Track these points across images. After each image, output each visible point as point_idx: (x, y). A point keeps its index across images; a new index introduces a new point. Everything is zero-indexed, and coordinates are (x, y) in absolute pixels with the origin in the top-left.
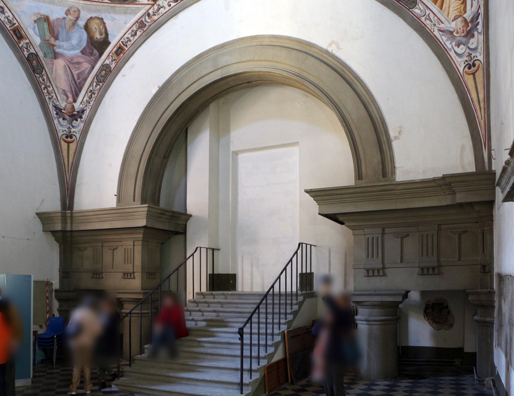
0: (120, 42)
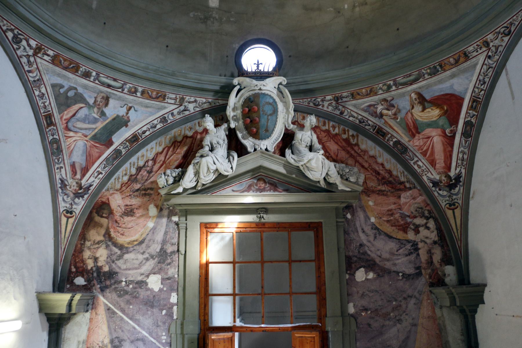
0: (137, 132)
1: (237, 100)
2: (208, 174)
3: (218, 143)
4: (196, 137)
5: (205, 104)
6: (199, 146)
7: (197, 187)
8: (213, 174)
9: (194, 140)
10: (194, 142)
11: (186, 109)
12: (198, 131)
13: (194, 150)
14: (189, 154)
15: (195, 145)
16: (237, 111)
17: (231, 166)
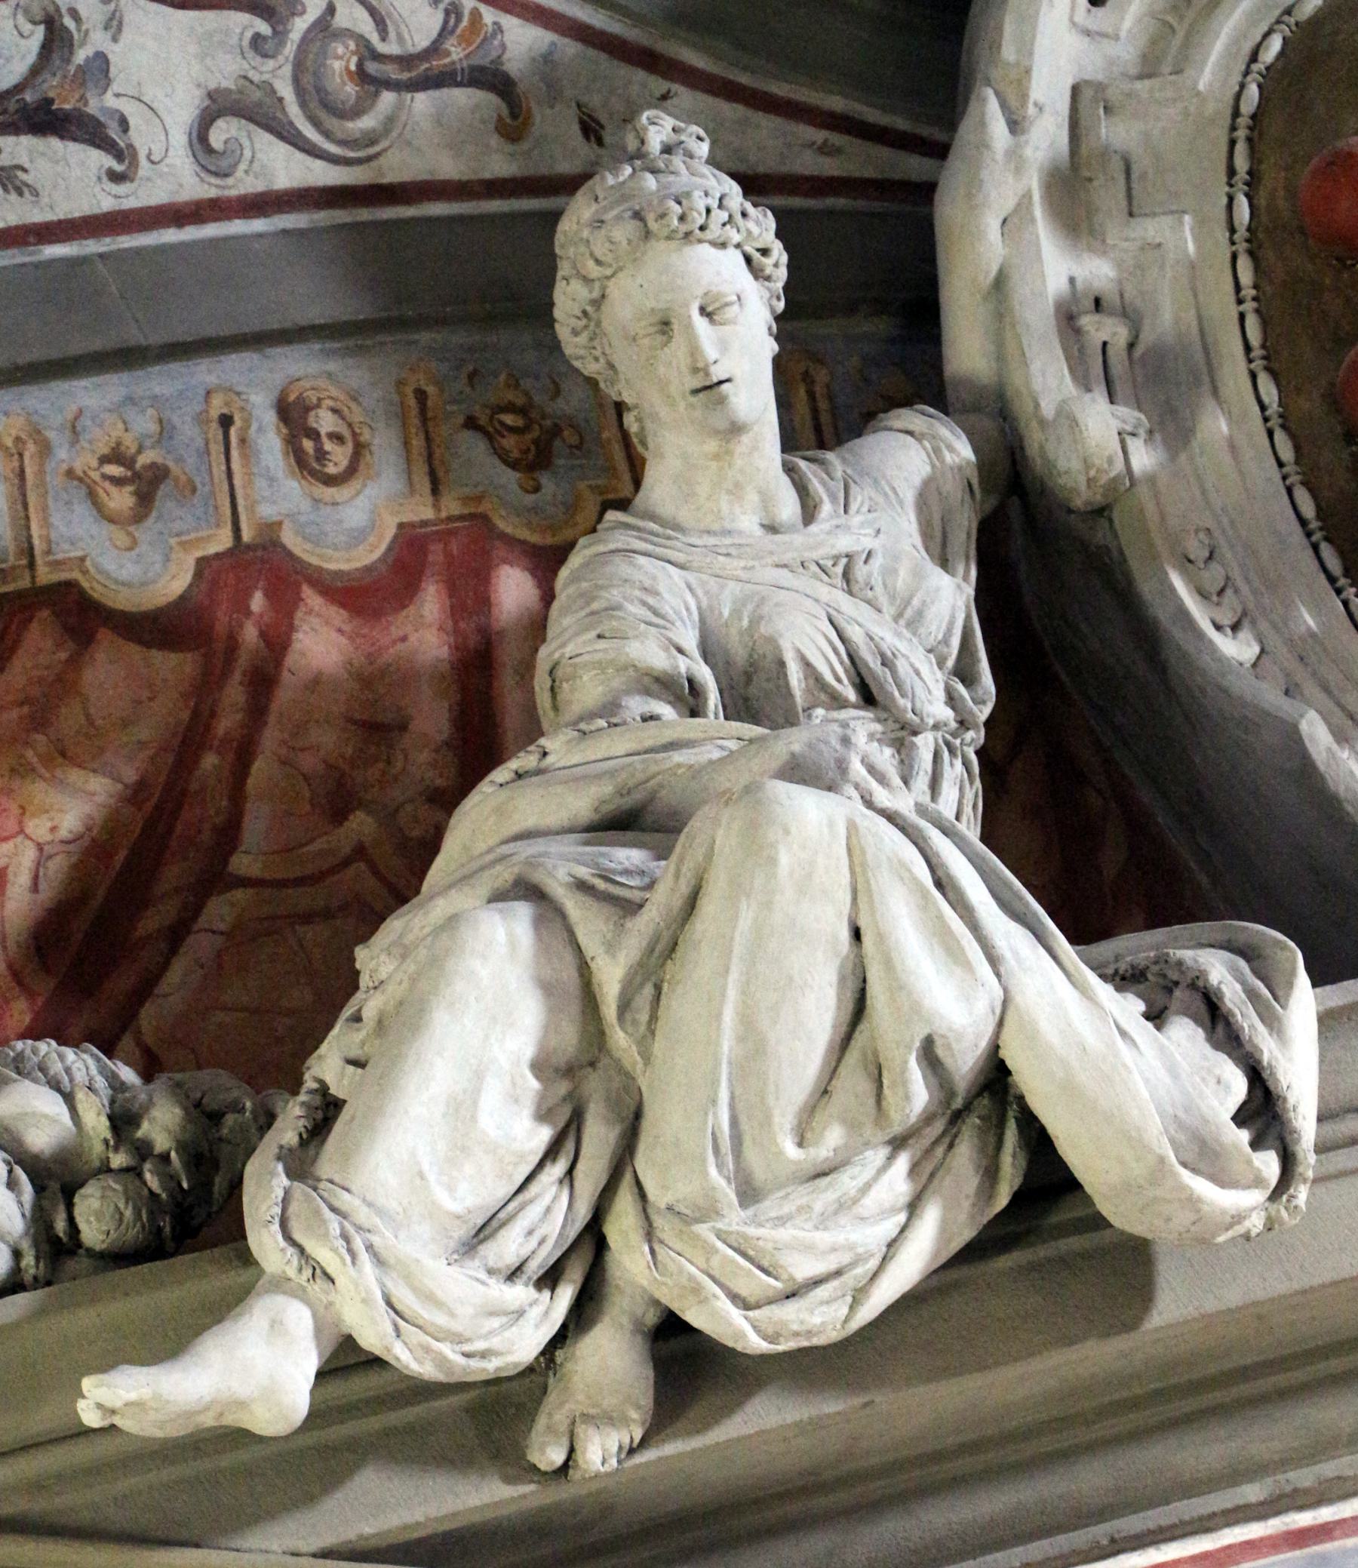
1: (1126, 52)
2: (832, 1138)
3: (868, 697)
4: (277, 642)
5: (422, 102)
6: (339, 815)
7: (554, 1413)
8: (897, 1182)
9: (235, 693)
10: (227, 722)
11: (50, 85)
12: (289, 538)
13: (243, 863)
14: (152, 922)
15: (261, 769)
16: (1151, 229)
17: (1238, 1086)
